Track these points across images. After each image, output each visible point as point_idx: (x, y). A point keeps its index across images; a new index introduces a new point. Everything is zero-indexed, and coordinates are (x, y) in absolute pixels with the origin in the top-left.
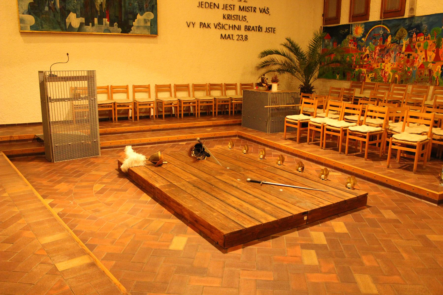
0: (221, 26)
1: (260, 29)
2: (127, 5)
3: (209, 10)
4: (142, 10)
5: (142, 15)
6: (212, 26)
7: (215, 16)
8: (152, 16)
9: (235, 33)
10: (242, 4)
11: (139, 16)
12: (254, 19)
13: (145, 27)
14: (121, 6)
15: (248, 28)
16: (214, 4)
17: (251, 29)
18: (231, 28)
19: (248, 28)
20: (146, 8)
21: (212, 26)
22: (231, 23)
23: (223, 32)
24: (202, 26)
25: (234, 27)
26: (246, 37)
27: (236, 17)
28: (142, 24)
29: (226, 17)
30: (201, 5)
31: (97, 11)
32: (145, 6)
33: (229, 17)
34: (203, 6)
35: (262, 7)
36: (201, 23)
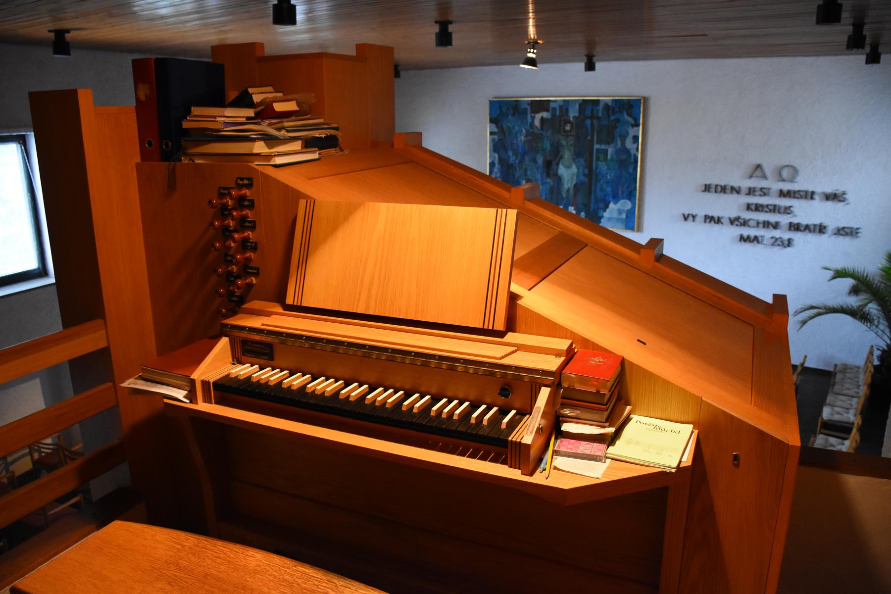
0: (742, 221)
1: (821, 229)
2: (598, 189)
3: (723, 197)
4: (616, 198)
5: (615, 203)
6: (726, 221)
7: (730, 206)
8: (628, 205)
9: (768, 234)
10: (786, 187)
11: (612, 205)
12: (804, 212)
13: (618, 220)
14: (590, 193)
15: (795, 227)
16: (732, 188)
17: (802, 228)
18: (761, 225)
19: (795, 227)
20: (623, 193)
21: (726, 221)
22: (762, 217)
23: (746, 231)
24: (708, 220)
25: (766, 224)
26: (789, 243)
27: (771, 208)
28: (615, 215)
29: (753, 207)
30: (707, 188)
31: (563, 198)
32: (620, 192)
33: (758, 208)
34: (713, 190)
35: (829, 190)
36: (706, 217)
